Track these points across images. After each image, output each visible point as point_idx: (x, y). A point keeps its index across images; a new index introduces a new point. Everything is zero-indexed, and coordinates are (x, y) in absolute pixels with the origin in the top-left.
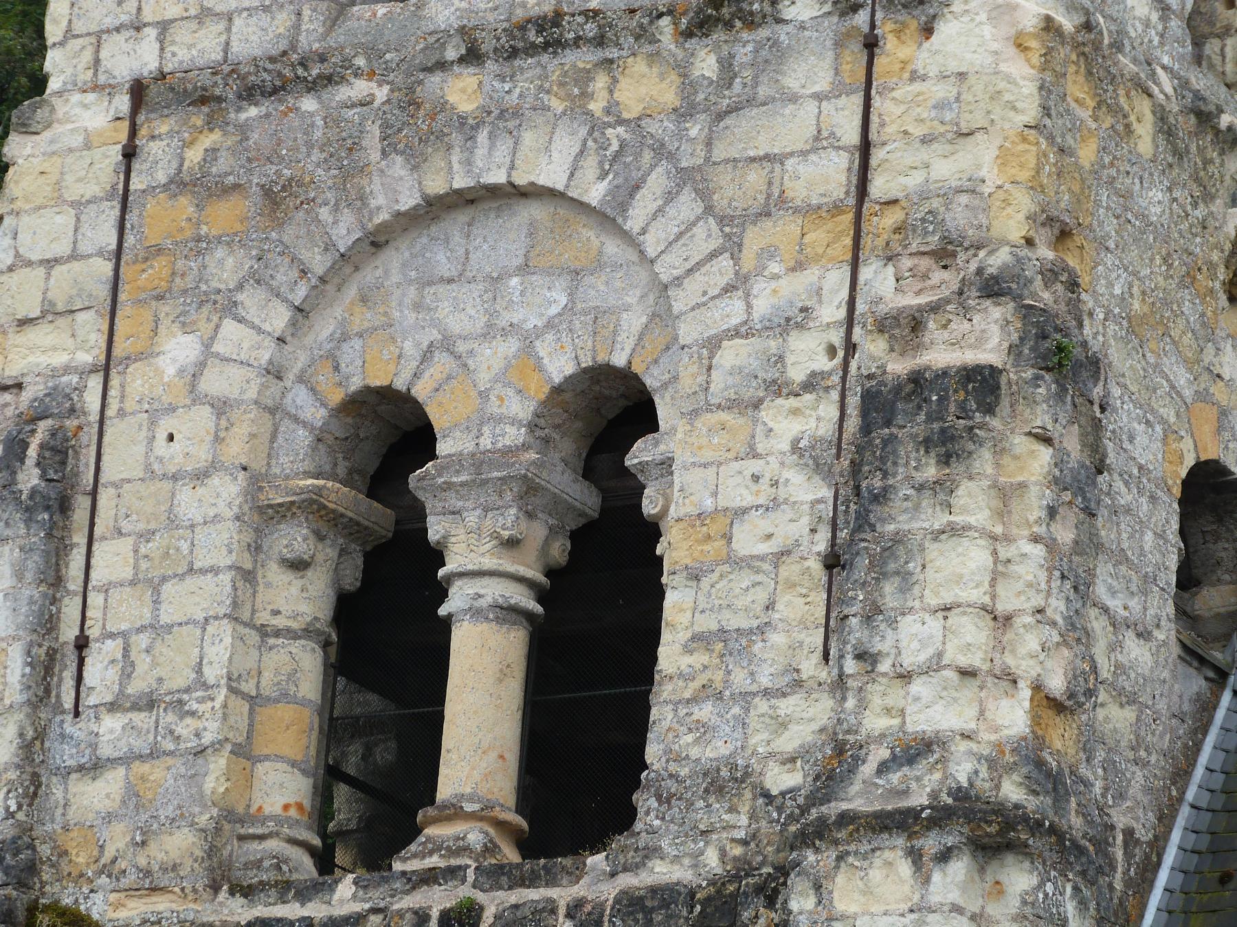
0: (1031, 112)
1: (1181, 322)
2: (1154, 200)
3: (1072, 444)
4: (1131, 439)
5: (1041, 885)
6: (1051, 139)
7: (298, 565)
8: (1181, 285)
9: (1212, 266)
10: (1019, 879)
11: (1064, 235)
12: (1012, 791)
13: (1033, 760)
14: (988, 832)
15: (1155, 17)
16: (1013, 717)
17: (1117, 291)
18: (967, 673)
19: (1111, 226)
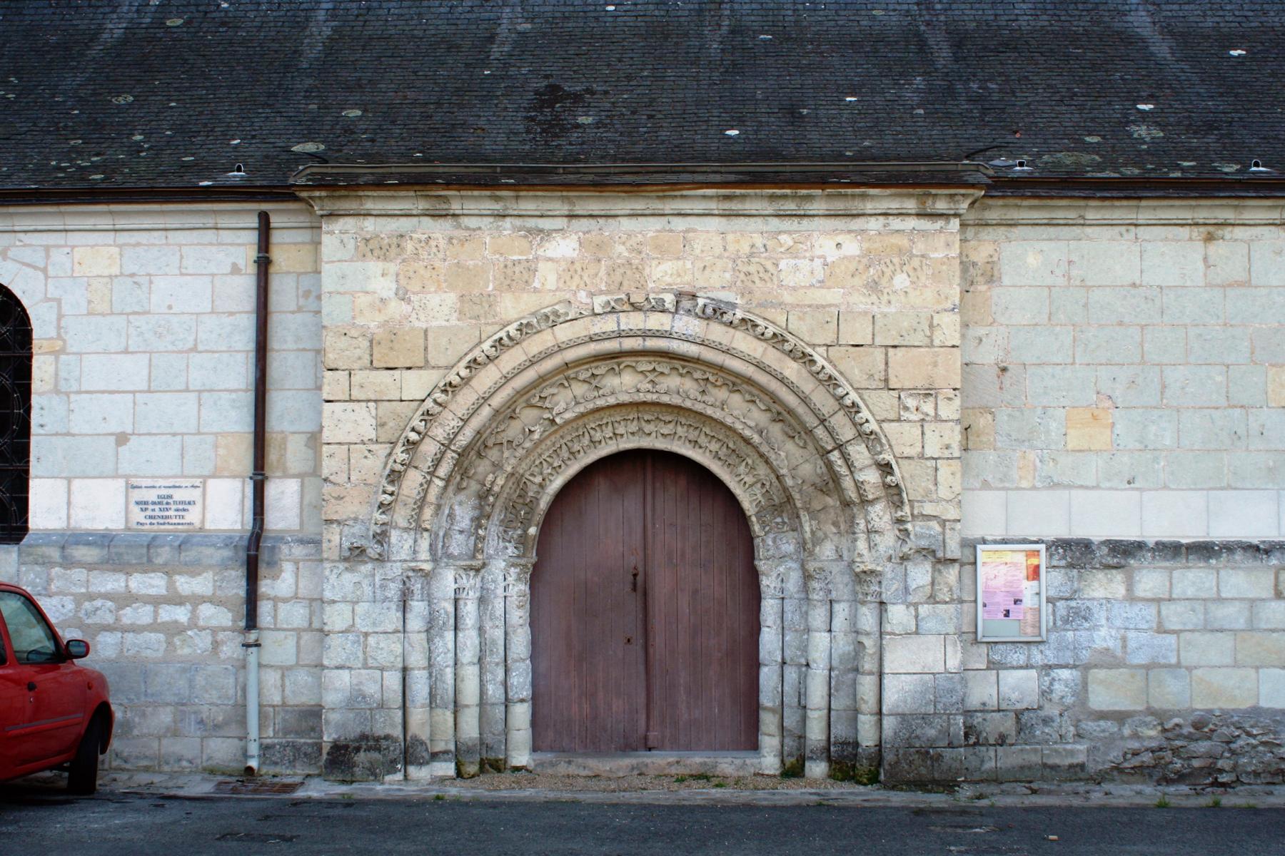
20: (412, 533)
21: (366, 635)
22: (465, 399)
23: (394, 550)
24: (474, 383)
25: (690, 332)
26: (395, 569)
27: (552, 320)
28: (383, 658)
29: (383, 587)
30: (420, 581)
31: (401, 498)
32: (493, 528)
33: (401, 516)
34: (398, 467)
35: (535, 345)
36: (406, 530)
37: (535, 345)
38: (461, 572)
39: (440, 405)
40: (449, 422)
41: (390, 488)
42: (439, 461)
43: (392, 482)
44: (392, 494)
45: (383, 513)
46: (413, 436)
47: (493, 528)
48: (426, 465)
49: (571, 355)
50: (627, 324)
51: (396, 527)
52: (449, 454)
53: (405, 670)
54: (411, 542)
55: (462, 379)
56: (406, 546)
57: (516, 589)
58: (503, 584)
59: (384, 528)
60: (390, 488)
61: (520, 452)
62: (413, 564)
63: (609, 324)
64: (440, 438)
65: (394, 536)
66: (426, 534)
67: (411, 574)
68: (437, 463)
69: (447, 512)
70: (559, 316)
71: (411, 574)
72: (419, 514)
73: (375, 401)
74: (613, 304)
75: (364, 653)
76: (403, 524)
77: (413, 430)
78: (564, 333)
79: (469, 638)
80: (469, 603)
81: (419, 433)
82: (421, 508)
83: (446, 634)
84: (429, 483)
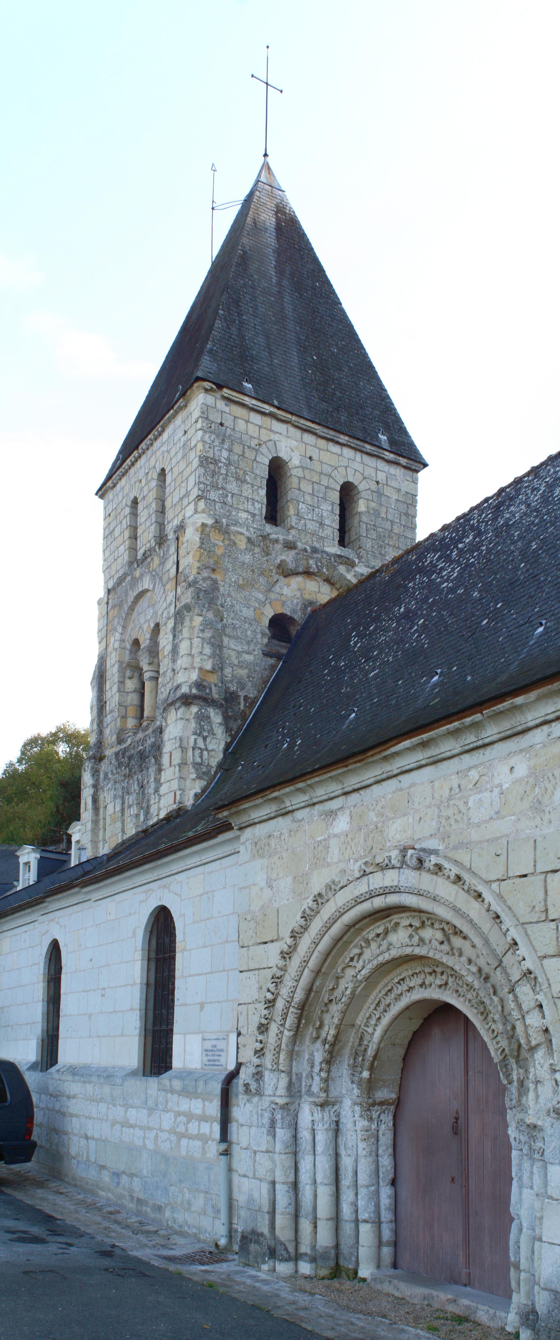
0: (198, 544)
1: (259, 584)
2: (247, 558)
3: (210, 615)
4: (241, 611)
5: (200, 710)
6: (205, 550)
7: (130, 678)
8: (259, 575)
9: (271, 571)
10: (194, 709)
11: (214, 570)
12: (194, 691)
13: (199, 685)
14: (187, 700)
15: (249, 517)
16: (194, 676)
17: (233, 580)
18: (186, 669)
19: (230, 566)
20: (276, 1073)
21: (255, 1152)
22: (296, 961)
23: (266, 1086)
24: (299, 949)
25: (409, 885)
26: (266, 1101)
27: (333, 888)
28: (261, 1172)
29: (262, 1115)
30: (280, 1111)
31: (269, 1045)
32: (343, 1070)
33: (268, 1060)
34: (264, 1021)
35: (327, 911)
36: (273, 1071)
37: (327, 911)
38: (313, 1107)
39: (281, 969)
40: (288, 982)
41: (260, 1037)
42: (286, 1014)
43: (262, 1033)
44: (261, 1042)
45: (258, 1057)
46: (269, 996)
47: (343, 1070)
48: (278, 1018)
49: (348, 918)
50: (373, 883)
51: (267, 1069)
52: (291, 1009)
53: (273, 1183)
54: (275, 1080)
55: (290, 947)
56: (272, 1084)
57: (361, 1124)
58: (352, 1120)
59: (260, 1069)
60: (260, 1037)
61: (340, 1006)
62: (272, 1098)
63: (361, 888)
64: (285, 997)
65: (267, 1074)
66: (283, 1075)
67: (274, 1107)
68: (285, 1017)
69: (307, 1057)
70: (336, 885)
71: (274, 1107)
72: (278, 1058)
73: (259, 969)
74: (363, 867)
75: (254, 1167)
76: (270, 1067)
77: (269, 991)
78: (342, 898)
79: (324, 1164)
80: (320, 1133)
81: (273, 994)
82: (279, 1053)
83: (306, 1157)
84: (282, 1032)
